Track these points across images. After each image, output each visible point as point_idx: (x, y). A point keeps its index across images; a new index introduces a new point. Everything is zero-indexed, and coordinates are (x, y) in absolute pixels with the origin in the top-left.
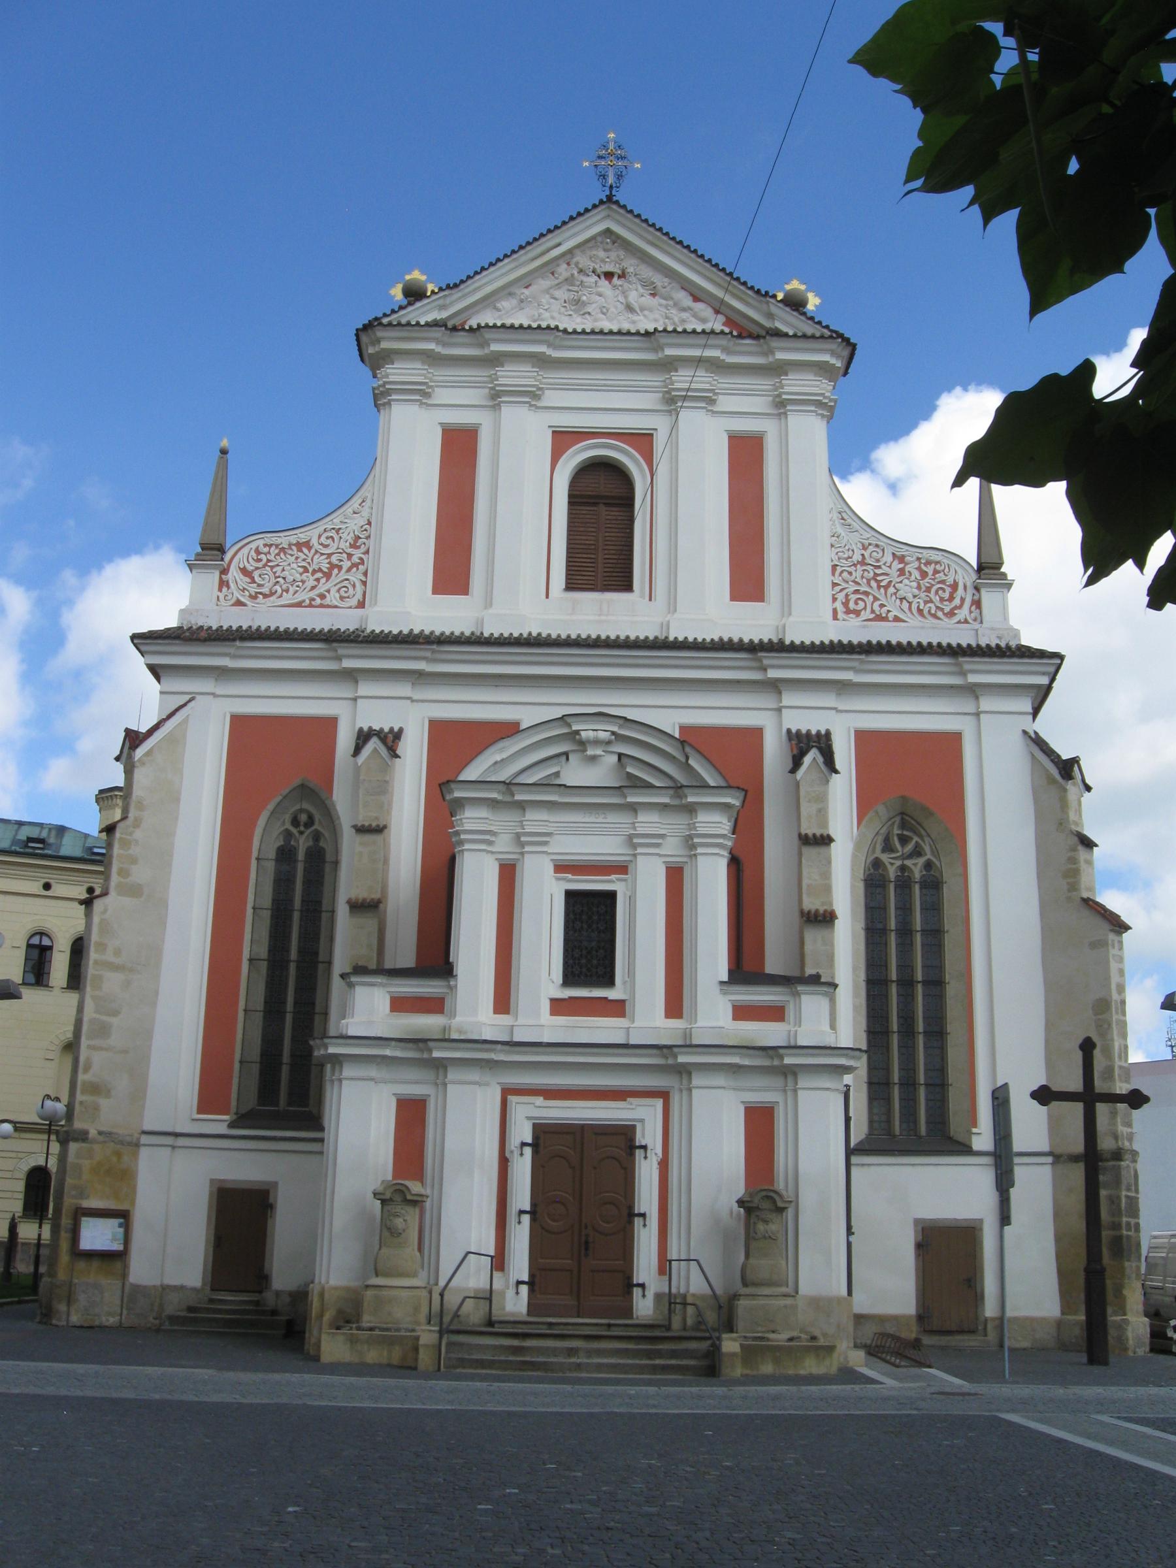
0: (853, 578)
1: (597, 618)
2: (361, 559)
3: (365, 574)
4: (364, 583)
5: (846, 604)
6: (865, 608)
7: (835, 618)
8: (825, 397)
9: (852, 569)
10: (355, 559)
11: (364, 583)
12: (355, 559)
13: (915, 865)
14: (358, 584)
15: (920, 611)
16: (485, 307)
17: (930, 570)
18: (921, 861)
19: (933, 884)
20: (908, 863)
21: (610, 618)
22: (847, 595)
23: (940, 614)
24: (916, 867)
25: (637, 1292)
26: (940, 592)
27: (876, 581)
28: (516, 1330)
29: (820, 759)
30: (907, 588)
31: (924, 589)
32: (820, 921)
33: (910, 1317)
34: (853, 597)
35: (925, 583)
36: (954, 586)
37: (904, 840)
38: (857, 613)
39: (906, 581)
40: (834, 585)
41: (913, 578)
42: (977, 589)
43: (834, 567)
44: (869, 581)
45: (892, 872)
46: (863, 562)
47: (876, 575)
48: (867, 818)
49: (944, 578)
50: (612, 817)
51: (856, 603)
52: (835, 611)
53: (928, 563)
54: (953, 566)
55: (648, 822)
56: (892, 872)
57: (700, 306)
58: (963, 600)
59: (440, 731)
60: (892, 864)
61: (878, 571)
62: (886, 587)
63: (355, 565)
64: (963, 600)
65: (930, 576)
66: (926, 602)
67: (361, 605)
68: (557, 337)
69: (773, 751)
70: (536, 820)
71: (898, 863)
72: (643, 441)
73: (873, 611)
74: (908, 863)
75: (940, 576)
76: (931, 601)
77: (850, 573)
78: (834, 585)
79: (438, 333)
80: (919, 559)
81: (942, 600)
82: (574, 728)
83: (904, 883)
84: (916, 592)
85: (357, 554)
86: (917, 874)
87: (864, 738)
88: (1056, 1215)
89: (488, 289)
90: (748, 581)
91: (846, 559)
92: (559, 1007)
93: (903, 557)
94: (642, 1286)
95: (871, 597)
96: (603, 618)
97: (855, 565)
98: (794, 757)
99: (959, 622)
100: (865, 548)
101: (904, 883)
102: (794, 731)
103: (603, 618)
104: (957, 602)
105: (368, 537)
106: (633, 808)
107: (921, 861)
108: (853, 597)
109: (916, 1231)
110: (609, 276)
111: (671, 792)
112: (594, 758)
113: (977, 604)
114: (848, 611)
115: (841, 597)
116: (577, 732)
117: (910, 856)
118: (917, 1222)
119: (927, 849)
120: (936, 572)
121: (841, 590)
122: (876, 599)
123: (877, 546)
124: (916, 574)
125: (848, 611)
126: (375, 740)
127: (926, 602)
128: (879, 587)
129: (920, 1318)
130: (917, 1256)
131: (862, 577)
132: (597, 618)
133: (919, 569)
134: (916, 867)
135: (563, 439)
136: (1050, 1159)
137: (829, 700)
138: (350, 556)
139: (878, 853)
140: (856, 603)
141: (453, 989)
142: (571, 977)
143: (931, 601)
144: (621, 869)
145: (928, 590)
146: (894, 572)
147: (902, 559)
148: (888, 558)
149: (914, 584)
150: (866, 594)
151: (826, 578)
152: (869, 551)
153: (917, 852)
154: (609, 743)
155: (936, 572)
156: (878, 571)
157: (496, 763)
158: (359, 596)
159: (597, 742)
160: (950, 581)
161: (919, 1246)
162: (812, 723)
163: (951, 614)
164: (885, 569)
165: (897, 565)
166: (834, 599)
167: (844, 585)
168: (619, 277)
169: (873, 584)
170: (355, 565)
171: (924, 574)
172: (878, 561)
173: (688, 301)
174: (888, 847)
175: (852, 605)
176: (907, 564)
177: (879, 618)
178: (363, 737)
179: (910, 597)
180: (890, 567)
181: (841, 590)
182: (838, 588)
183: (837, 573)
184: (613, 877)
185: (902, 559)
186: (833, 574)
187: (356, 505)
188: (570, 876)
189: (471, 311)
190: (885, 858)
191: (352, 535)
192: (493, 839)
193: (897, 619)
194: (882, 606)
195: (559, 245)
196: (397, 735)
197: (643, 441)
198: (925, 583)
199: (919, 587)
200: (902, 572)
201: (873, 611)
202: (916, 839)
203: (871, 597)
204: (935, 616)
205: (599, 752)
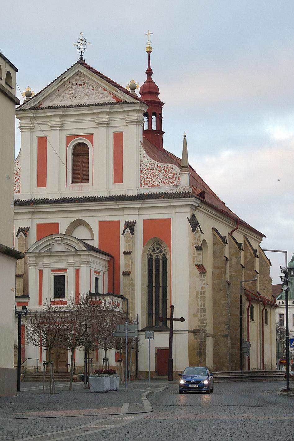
0: (146, 174)
1: (78, 192)
2: (18, 178)
3: (20, 183)
4: (20, 185)
5: (144, 182)
6: (149, 183)
7: (141, 186)
8: (138, 120)
9: (146, 171)
10: (17, 179)
11: (20, 185)
12: (17, 179)
13: (160, 255)
14: (18, 186)
15: (164, 182)
16: (47, 99)
17: (167, 170)
18: (162, 253)
19: (165, 261)
20: (158, 254)
21: (82, 191)
22: (145, 179)
23: (169, 183)
24: (160, 256)
25: (69, 366)
26: (170, 176)
27: (153, 174)
28: (39, 374)
29: (129, 231)
30: (161, 176)
31: (165, 175)
32: (126, 275)
33: (153, 371)
34: (146, 180)
36: (174, 174)
37: (158, 248)
38: (147, 184)
39: (161, 174)
40: (141, 176)
41: (162, 173)
42: (180, 174)
43: (141, 171)
44: (150, 174)
45: (154, 258)
46: (149, 169)
47: (153, 172)
48: (146, 244)
49: (171, 172)
50: (63, 258)
51: (147, 181)
52: (141, 184)
53: (167, 168)
54: (174, 168)
55: (71, 259)
56: (154, 258)
57: (106, 92)
58: (176, 178)
59: (40, 227)
60: (154, 255)
61: (153, 171)
62: (155, 176)
63: (17, 180)
64: (176, 178)
65: (167, 171)
66: (166, 179)
67: (19, 192)
68: (64, 110)
69: (122, 226)
70: (46, 260)
71: (156, 255)
72: (90, 137)
73: (151, 183)
74: (158, 254)
75: (170, 171)
76: (167, 179)
77: (146, 173)
78: (141, 176)
79: (33, 111)
80: (164, 167)
81: (170, 178)
82: (53, 237)
83: (157, 260)
84: (163, 176)
85: (18, 177)
86: (160, 257)
87: (145, 221)
88: (189, 347)
89: (47, 94)
90: (118, 177)
91: (145, 168)
92: (53, 303)
93: (160, 166)
94: (70, 365)
95: (151, 179)
96: (80, 191)
97: (147, 170)
98: (124, 230)
99: (174, 185)
100: (150, 165)
101: (157, 260)
102: (127, 221)
103: (80, 191)
104: (174, 179)
105: (20, 172)
106: (67, 256)
107: (162, 254)
108: (146, 180)
109: (155, 351)
110: (81, 85)
111: (75, 252)
112: (59, 244)
113: (179, 179)
114: (145, 184)
115: (143, 180)
116: (54, 238)
117: (159, 253)
118: (155, 348)
120: (169, 170)
121: (143, 178)
122: (152, 180)
123: (153, 164)
124: (163, 171)
125: (145, 184)
126: (21, 233)
127: (166, 179)
128: (153, 177)
129: (156, 372)
130: (156, 356)
131: (149, 173)
132: (78, 192)
133: (164, 169)
134: (160, 256)
135: (70, 138)
136: (188, 332)
137: (136, 212)
138: (16, 177)
139: (151, 253)
140: (147, 181)
141: (29, 300)
142: (55, 297)
143: (167, 179)
144: (66, 270)
145: (167, 176)
146: (157, 171)
147: (160, 167)
148: (156, 167)
149: (163, 174)
150: (150, 178)
152: (151, 166)
153: (161, 251)
154: (62, 240)
155: (169, 170)
156: (153, 171)
157: (36, 247)
158: (19, 189)
159: (59, 240)
160: (173, 173)
161: (156, 354)
162: (131, 219)
163: (173, 182)
164: (155, 170)
166: (141, 181)
167: (144, 176)
168: (84, 85)
169: (152, 175)
170: (17, 180)
171: (166, 171)
172: (153, 168)
173: (103, 91)
174: (154, 251)
175: (146, 182)
176: (161, 168)
177: (153, 185)
178: (20, 230)
179: (161, 178)
180: (156, 170)
181: (143, 178)
182: (142, 177)
183: (142, 173)
184: (64, 272)
186: (141, 173)
187: (17, 162)
188: (54, 272)
189: (43, 101)
190: (152, 253)
191: (16, 171)
192: (37, 265)
193: (158, 185)
194: (154, 182)
195: (65, 77)
196: (28, 229)
197: (90, 137)
198: (166, 174)
199: (164, 175)
200: (160, 171)
201: (151, 183)
202: (161, 248)
203: (151, 179)
204: (168, 183)
205: (60, 243)
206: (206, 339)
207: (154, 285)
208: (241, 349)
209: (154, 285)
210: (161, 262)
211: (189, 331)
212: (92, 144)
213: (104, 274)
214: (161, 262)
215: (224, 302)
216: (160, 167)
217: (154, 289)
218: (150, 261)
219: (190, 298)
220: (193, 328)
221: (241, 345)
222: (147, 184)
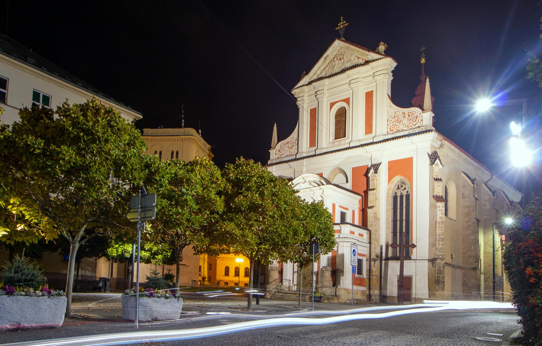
19: (408, 196)
20: (402, 192)
35: (409, 118)
37: (402, 186)
45: (399, 194)
56: (399, 194)
101: (402, 196)
107: (405, 191)
114: (391, 131)
115: (389, 128)
119: (407, 188)
125: (391, 131)
151: (385, 123)
153: (405, 189)
165: (403, 115)
174: (398, 188)
185: (404, 113)
190: (397, 191)
200: (404, 117)
206: (444, 268)
207: (398, 218)
208: (494, 282)
209: (398, 218)
210: (404, 198)
211: (429, 260)
212: (349, 105)
213: (353, 212)
214: (404, 198)
215: (473, 238)
216: (404, 113)
217: (398, 222)
218: (395, 198)
219: (429, 229)
220: (431, 258)
221: (494, 278)
222: (393, 130)
